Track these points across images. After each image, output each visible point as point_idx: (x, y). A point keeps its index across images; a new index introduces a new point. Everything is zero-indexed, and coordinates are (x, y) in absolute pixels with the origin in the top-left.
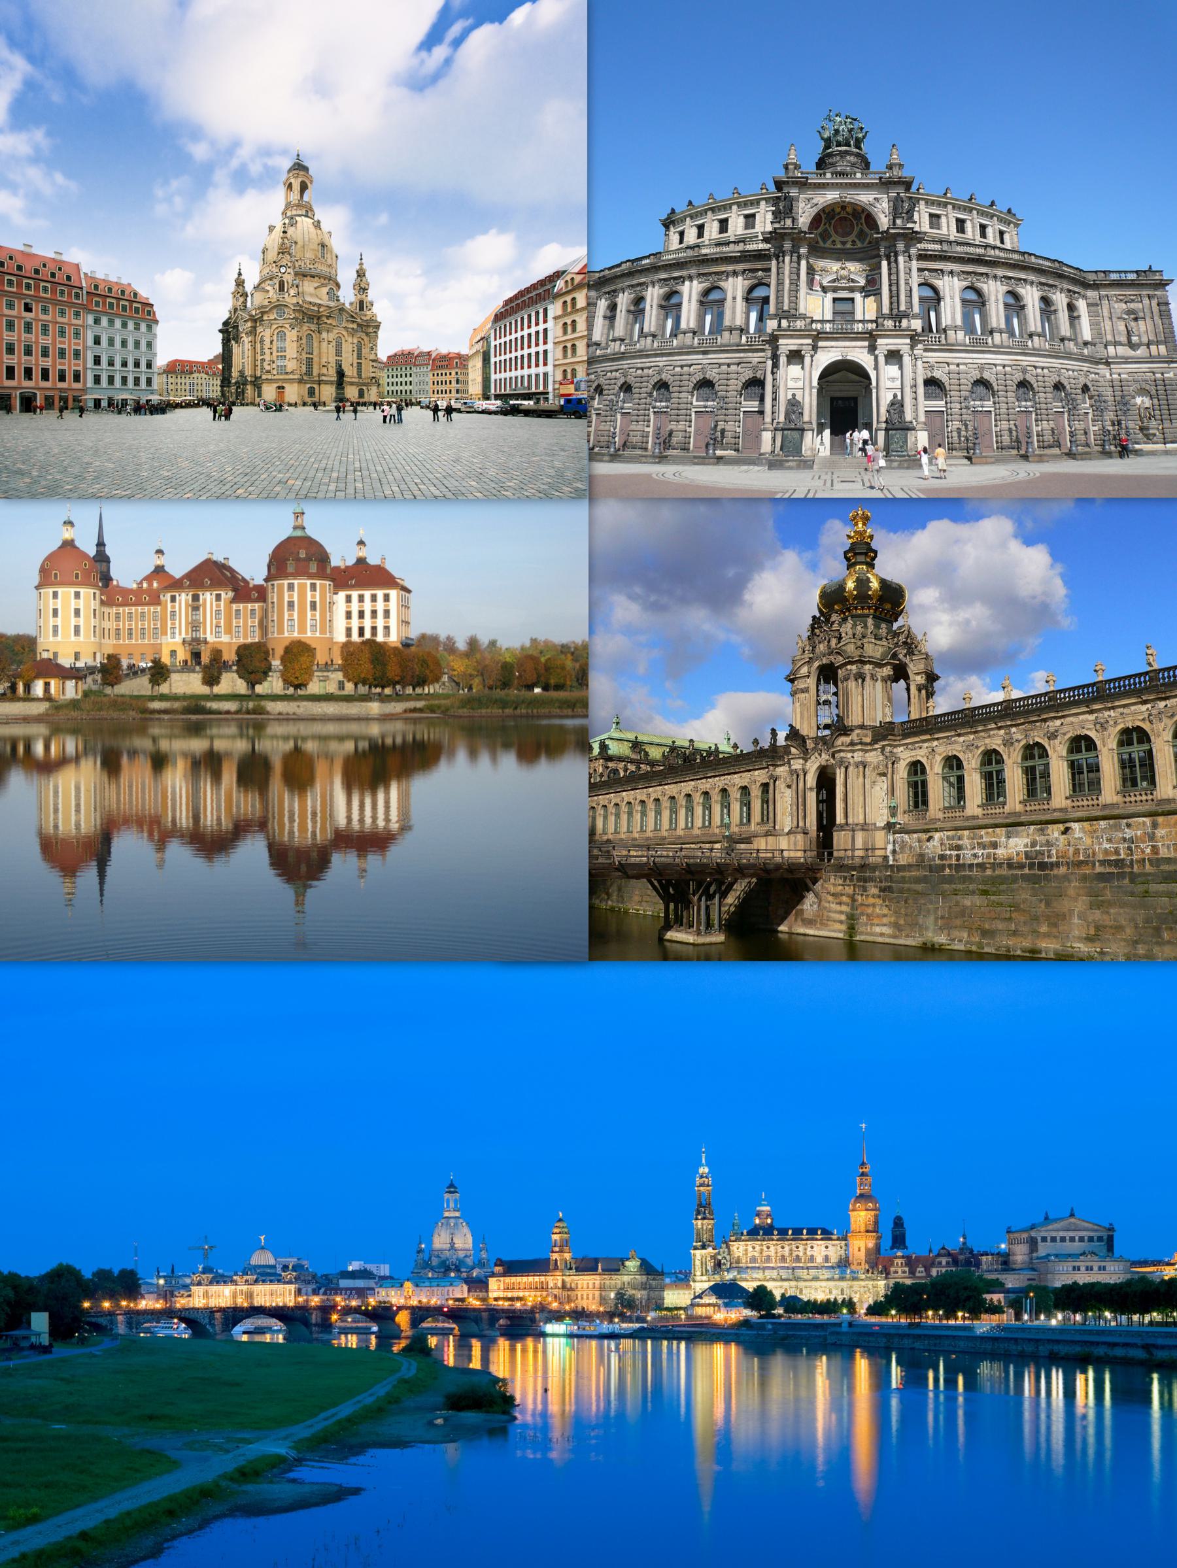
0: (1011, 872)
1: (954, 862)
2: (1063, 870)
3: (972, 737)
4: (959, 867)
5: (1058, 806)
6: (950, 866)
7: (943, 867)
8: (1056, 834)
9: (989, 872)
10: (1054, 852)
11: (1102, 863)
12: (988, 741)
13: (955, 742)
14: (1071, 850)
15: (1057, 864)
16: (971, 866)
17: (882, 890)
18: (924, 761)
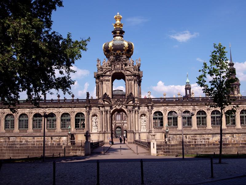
0: (214, 146)
1: (194, 143)
2: (231, 146)
3: (181, 107)
4: (196, 145)
5: (209, 129)
6: (193, 145)
7: (190, 145)
8: (228, 136)
9: (207, 146)
10: (227, 141)
11: (242, 144)
12: (187, 108)
13: (176, 107)
14: (233, 140)
15: (229, 144)
16: (200, 145)
17: (164, 152)
18: (162, 112)
